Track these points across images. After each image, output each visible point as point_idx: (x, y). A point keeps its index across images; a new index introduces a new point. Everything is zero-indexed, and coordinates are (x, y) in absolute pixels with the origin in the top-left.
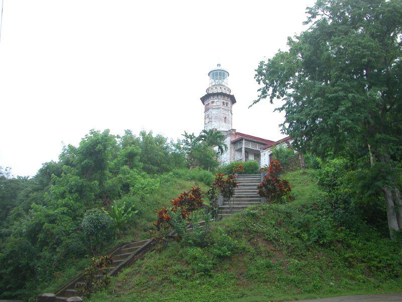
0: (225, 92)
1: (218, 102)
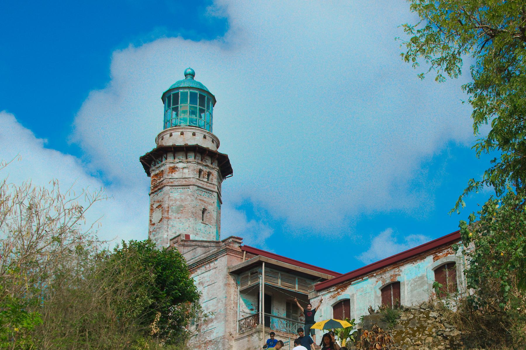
1: (186, 169)
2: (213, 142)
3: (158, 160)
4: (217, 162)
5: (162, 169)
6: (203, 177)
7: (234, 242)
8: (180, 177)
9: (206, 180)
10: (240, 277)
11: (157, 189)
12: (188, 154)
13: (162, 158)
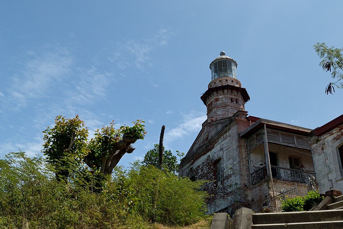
1: (223, 98)
3: (209, 97)
4: (240, 93)
5: (211, 100)
8: (221, 103)
10: (249, 140)
12: (224, 91)
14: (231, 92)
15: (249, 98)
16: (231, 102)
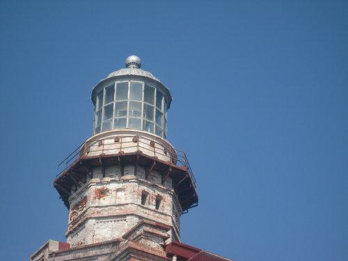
0: (151, 154)
2: (166, 153)
3: (80, 183)
6: (149, 204)
7: (149, 235)
8: (112, 203)
9: (154, 208)
11: (76, 225)
13: (86, 177)
14: (144, 176)
15: (195, 200)
16: (143, 202)
